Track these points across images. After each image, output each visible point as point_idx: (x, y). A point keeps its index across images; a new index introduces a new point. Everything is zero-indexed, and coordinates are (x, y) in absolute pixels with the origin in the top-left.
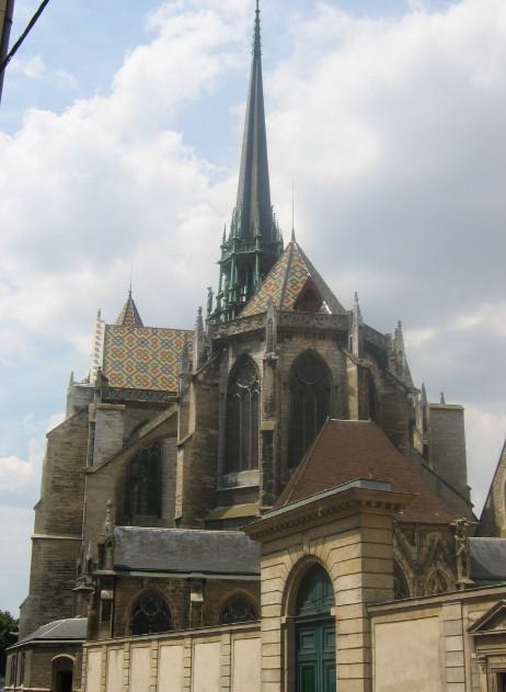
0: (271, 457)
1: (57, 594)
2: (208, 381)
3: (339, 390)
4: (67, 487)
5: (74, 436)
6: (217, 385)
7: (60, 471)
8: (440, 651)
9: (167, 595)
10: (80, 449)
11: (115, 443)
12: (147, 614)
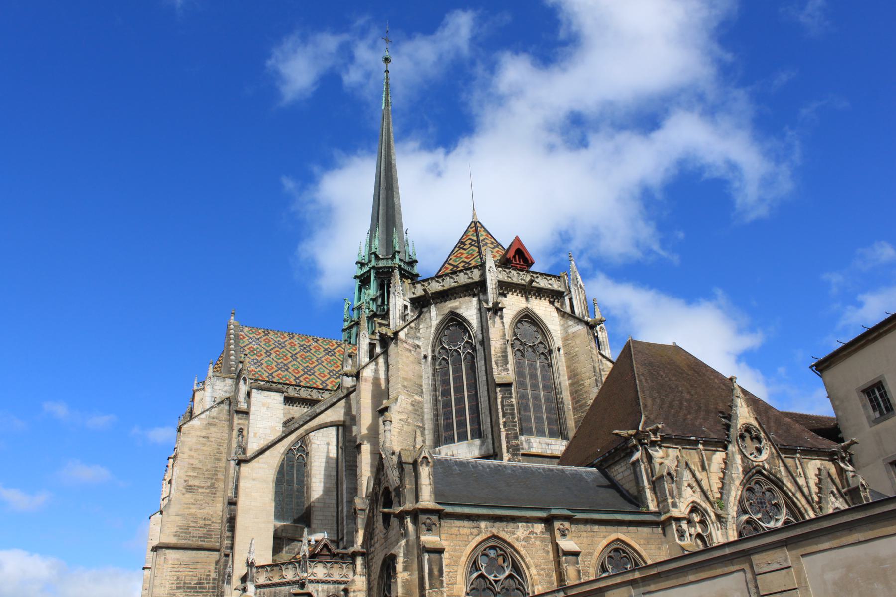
0: (513, 414)
4: (203, 487)
5: (212, 429)
6: (418, 346)
9: (517, 545)
11: (273, 429)
12: (491, 578)
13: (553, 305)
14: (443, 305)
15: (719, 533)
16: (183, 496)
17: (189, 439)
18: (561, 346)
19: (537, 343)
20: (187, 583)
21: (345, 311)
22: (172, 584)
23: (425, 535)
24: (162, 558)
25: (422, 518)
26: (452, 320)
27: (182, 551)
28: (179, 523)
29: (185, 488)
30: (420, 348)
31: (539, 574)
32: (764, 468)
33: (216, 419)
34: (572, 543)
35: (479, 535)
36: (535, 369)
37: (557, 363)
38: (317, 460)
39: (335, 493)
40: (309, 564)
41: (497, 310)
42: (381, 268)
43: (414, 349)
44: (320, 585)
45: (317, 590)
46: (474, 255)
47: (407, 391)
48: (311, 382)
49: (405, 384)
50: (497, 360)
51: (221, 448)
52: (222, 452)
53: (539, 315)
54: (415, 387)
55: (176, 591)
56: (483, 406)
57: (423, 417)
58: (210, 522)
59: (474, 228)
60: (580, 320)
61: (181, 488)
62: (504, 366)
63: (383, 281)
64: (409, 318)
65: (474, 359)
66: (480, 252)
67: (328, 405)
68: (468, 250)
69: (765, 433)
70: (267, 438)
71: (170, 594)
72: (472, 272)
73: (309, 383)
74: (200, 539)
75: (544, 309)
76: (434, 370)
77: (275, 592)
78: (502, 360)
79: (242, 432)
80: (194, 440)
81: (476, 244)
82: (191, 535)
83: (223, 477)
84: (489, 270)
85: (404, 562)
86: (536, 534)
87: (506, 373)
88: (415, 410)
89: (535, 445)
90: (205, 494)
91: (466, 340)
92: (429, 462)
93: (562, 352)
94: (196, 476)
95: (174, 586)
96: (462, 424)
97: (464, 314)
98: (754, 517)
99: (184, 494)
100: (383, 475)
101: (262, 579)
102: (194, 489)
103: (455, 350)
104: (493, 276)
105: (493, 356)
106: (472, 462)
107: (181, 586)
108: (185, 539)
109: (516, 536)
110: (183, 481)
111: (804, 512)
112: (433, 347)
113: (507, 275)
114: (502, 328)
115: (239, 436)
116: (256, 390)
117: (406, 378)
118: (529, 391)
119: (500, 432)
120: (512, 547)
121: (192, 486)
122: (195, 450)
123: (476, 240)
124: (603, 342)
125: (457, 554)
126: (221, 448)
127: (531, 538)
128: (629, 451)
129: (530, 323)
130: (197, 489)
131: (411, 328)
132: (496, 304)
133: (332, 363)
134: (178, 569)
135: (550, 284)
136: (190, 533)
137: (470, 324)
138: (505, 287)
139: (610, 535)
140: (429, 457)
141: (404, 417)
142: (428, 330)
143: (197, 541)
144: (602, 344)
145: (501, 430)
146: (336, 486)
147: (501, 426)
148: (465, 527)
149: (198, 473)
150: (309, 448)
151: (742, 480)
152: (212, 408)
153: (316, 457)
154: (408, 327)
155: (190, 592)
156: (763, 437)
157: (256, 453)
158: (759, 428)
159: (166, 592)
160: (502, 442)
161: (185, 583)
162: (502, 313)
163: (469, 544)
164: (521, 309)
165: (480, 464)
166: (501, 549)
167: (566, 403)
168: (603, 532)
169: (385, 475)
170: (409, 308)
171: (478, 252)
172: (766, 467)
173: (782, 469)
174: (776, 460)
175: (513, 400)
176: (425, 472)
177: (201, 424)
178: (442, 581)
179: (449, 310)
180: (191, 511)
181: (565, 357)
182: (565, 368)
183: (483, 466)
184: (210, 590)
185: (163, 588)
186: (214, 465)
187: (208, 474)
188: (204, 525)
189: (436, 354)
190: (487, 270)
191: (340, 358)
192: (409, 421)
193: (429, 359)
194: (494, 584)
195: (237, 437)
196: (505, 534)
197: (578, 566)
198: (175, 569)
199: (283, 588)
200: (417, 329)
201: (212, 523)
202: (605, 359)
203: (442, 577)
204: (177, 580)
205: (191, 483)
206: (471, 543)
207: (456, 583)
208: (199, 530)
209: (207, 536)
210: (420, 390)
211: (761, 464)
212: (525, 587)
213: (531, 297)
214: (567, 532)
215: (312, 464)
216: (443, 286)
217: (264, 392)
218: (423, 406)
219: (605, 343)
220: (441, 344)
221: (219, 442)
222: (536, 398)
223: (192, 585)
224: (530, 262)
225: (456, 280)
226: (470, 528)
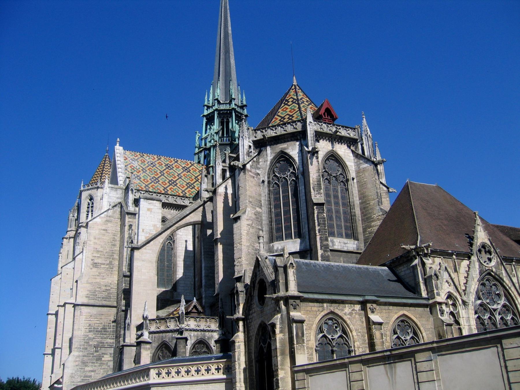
0: (324, 224)
1: (96, 351)
4: (104, 264)
5: (109, 225)
6: (258, 174)
9: (345, 318)
12: (330, 337)
13: (350, 148)
14: (275, 146)
15: (464, 311)
16: (91, 270)
17: (94, 232)
18: (355, 177)
19: (338, 174)
20: (96, 329)
21: (196, 140)
22: (86, 329)
23: (293, 311)
24: (79, 312)
25: (291, 301)
26: (282, 157)
27: (91, 307)
28: (89, 289)
29: (92, 265)
30: (260, 175)
31: (358, 335)
32: (492, 271)
33: (112, 217)
34: (378, 316)
35: (323, 311)
36: (337, 192)
37: (352, 188)
38: (180, 246)
39: (193, 268)
40: (185, 318)
41: (314, 152)
42: (222, 110)
43: (256, 176)
44: (192, 332)
45: (190, 336)
46: (295, 110)
47: (252, 205)
48: (175, 191)
49: (251, 200)
50: (314, 187)
51: (116, 237)
52: (116, 240)
53: (341, 155)
54: (256, 202)
55: (89, 333)
56: (303, 217)
57: (262, 222)
58: (109, 288)
59: (294, 90)
60: (368, 160)
62: (319, 191)
63: (223, 119)
65: (297, 184)
66: (299, 108)
68: (290, 106)
71: (85, 336)
72: (296, 124)
73: (174, 192)
74: (103, 299)
75: (344, 151)
76: (269, 190)
77: (162, 337)
79: (131, 227)
80: (97, 232)
81: (297, 102)
82: (97, 296)
83: (118, 257)
84: (309, 124)
86: (356, 311)
87: (320, 196)
88: (257, 218)
89: (337, 244)
91: (291, 171)
92: (294, 266)
93: (355, 181)
94: (99, 257)
95: (87, 330)
96: (288, 228)
97: (290, 153)
99: (91, 269)
100: (259, 271)
101: (153, 328)
102: (98, 265)
103: (284, 178)
104: (312, 128)
105: (311, 184)
106: (313, 263)
107: (91, 330)
108: (93, 299)
109: (344, 312)
110: (90, 260)
111: (515, 299)
112: (269, 174)
113: (320, 127)
114: (317, 165)
115: (129, 230)
116: (143, 199)
117: (251, 196)
118: (333, 207)
119: (316, 236)
121: (97, 264)
122: (98, 238)
123: (296, 99)
124: (381, 173)
125: (310, 323)
126: (116, 237)
127: (353, 313)
128: (410, 258)
130: (100, 266)
131: (254, 161)
132: (314, 149)
133: (188, 177)
134: (89, 319)
135: (348, 134)
137: (294, 160)
138: (319, 136)
139: (399, 312)
140: (294, 263)
142: (265, 163)
143: (101, 300)
144: (380, 174)
145: (317, 235)
146: (193, 264)
147: (317, 232)
149: (100, 254)
151: (479, 279)
152: (109, 210)
153: (180, 244)
154: (252, 161)
156: (492, 251)
157: (144, 243)
159: (82, 334)
160: (317, 242)
161: (94, 328)
162: (318, 155)
163: (317, 316)
165: (317, 264)
166: (336, 320)
167: (357, 216)
168: (395, 310)
169: (260, 272)
170: (252, 147)
171: (298, 108)
173: (504, 272)
174: (500, 266)
175: (325, 215)
176: (291, 272)
177: (101, 221)
178: (303, 340)
179: (280, 150)
180: (96, 280)
181: (357, 184)
183: (319, 266)
184: (111, 333)
185: (80, 332)
186: (111, 249)
187: (108, 255)
188: (106, 289)
189: (271, 179)
190: (308, 124)
191: (193, 174)
193: (266, 183)
194: (332, 341)
195: (128, 230)
196: (338, 310)
197: (381, 331)
198: (87, 319)
199: (168, 334)
200: (258, 162)
201: (111, 288)
202: (381, 185)
203: (304, 337)
204: (89, 326)
205: (96, 261)
206: (319, 316)
207: (310, 340)
208: (102, 293)
209: (108, 298)
211: (490, 268)
212: (350, 343)
213: (336, 143)
214: (374, 310)
215: (177, 249)
216: (276, 133)
217: (148, 200)
219: (382, 174)
220: (274, 173)
221: (114, 233)
222: (337, 212)
223: (99, 330)
224: (335, 118)
225: (285, 129)
226: (318, 307)
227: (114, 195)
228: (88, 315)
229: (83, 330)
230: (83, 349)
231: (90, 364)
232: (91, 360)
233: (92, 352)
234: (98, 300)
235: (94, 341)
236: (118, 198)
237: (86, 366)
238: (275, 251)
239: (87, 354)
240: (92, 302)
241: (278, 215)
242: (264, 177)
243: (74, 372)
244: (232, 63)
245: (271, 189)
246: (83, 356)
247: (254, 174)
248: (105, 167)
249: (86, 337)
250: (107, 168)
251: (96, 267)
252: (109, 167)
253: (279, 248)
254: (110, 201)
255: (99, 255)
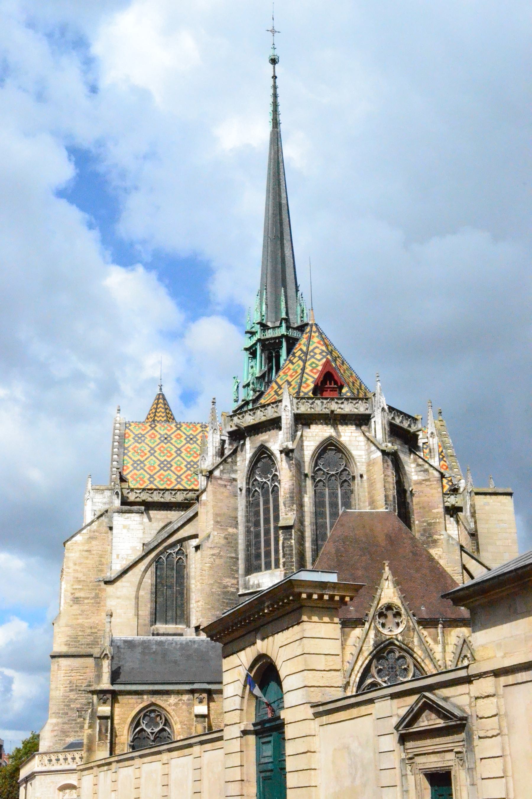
0: (291, 555)
2: (225, 476)
3: (365, 477)
4: (88, 598)
5: (94, 543)
6: (235, 480)
7: (79, 582)
8: (375, 753)
9: (168, 709)
10: (101, 556)
12: (149, 731)
16: (71, 608)
19: (340, 470)
20: (79, 686)
22: (66, 687)
23: (101, 706)
31: (182, 728)
32: (397, 640)
33: (97, 532)
36: (337, 497)
37: (358, 489)
42: (268, 339)
43: (229, 484)
47: (221, 526)
50: (285, 501)
51: (103, 559)
54: (229, 521)
57: (237, 547)
58: (96, 630)
61: (68, 601)
63: (271, 353)
64: (227, 452)
67: (186, 520)
69: (406, 610)
70: (129, 558)
75: (350, 434)
78: (290, 500)
80: (77, 554)
85: (89, 723)
86: (184, 701)
87: (292, 513)
88: (229, 543)
90: (90, 604)
94: (81, 589)
95: (68, 689)
98: (379, 680)
99: (71, 606)
103: (265, 483)
108: (75, 647)
109: (168, 703)
110: (69, 594)
112: (249, 478)
113: (310, 406)
116: (117, 514)
120: (166, 710)
125: (125, 716)
126: (103, 559)
129: (335, 450)
134: (70, 674)
136: (79, 641)
141: (216, 551)
143: (85, 648)
148: (132, 699)
150: (188, 551)
151: (372, 651)
152: (93, 522)
155: (82, 693)
158: (400, 606)
159: (61, 694)
161: (76, 686)
164: (324, 438)
170: (227, 442)
172: (399, 639)
173: (416, 640)
175: (293, 541)
177: (83, 538)
180: (78, 621)
182: (367, 494)
185: (58, 692)
187: (94, 586)
188: (92, 633)
189: (250, 487)
192: (222, 553)
193: (244, 491)
198: (67, 675)
200: (235, 462)
201: (98, 630)
202: (432, 469)
205: (77, 595)
207: (122, 735)
210: (234, 523)
211: (394, 637)
216: (254, 419)
217: (124, 514)
218: (238, 537)
221: (101, 555)
226: (136, 699)
227: (100, 500)
228: (68, 668)
229: (62, 689)
230: (63, 714)
231: (73, 733)
232: (74, 728)
233: (74, 718)
234: (82, 648)
235: (77, 704)
236: (105, 504)
237: (67, 736)
238: (250, 587)
239: (68, 721)
240: (73, 651)
241: (258, 535)
242: (242, 483)
243: (51, 744)
244: (287, 255)
245: (251, 499)
246: (63, 723)
247: (226, 481)
248: (157, 414)
249: (66, 699)
250: (160, 416)
251: (78, 604)
252: (163, 413)
253: (256, 583)
254: (95, 508)
255: (80, 587)
